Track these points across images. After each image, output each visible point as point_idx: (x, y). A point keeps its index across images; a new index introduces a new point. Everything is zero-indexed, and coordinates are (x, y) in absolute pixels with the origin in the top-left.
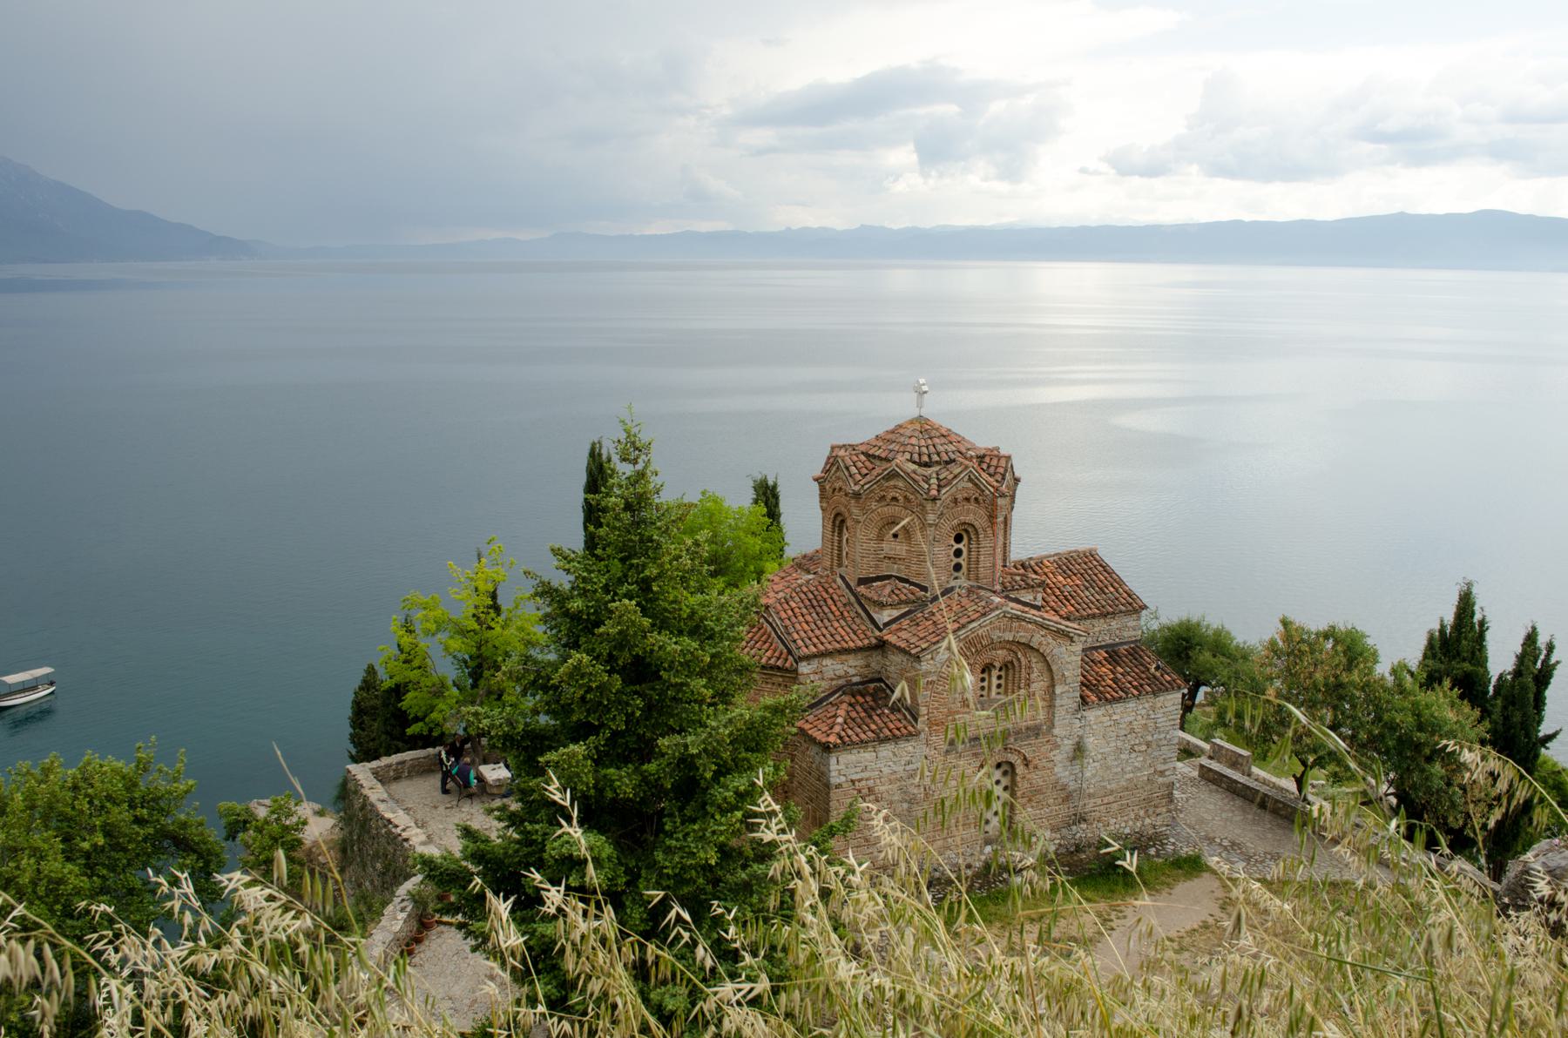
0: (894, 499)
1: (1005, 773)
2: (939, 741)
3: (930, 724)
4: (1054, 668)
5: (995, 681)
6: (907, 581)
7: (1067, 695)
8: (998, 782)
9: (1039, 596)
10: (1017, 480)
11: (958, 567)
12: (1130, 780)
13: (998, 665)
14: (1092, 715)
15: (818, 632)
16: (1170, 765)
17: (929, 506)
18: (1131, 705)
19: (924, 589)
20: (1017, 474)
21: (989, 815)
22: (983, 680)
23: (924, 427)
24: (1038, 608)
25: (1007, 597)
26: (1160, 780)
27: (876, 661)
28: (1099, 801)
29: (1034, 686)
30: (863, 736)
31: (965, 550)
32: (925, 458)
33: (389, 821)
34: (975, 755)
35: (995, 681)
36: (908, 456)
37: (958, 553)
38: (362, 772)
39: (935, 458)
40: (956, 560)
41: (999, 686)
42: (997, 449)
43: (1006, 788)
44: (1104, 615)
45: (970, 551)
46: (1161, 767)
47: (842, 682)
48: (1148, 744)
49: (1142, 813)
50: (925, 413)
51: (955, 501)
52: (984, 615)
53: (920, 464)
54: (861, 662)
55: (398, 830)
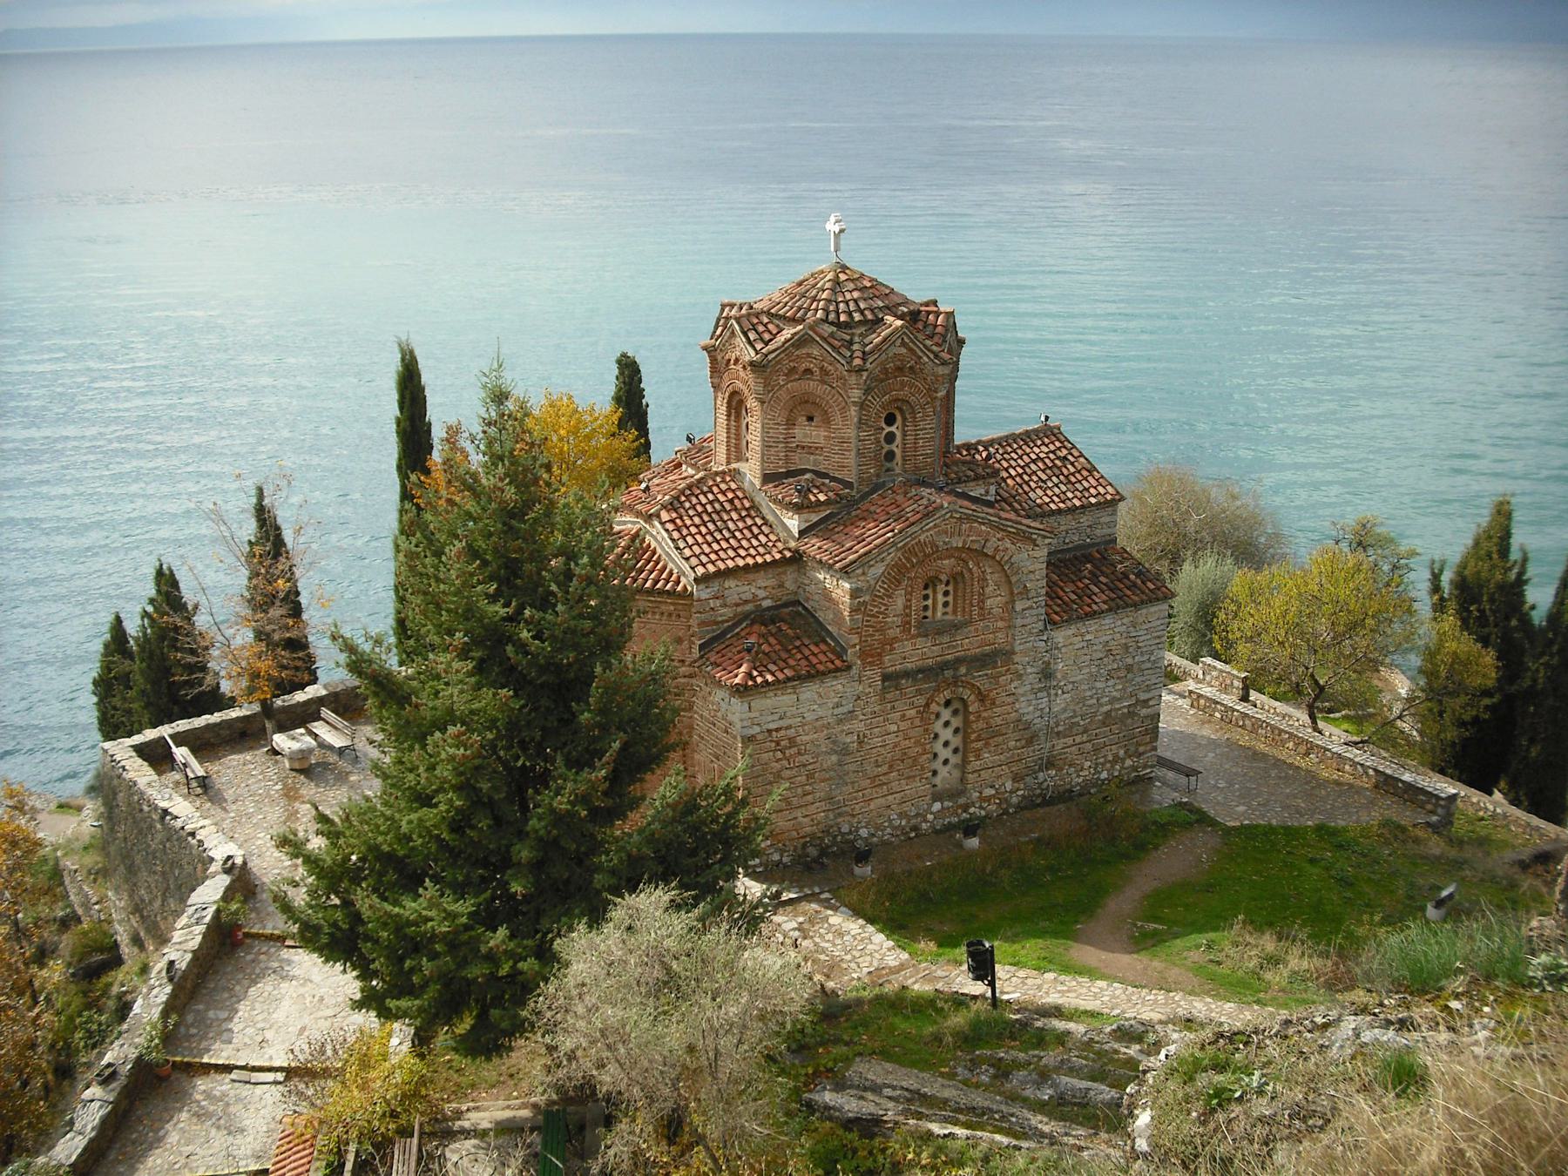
0: (808, 371)
1: (955, 712)
2: (874, 674)
3: (863, 655)
4: (1014, 579)
5: (941, 599)
6: (825, 475)
7: (1031, 612)
8: (947, 724)
9: (992, 489)
10: (961, 342)
11: (890, 456)
13: (944, 578)
14: (1060, 636)
15: (716, 546)
16: (1156, 693)
17: (853, 380)
18: (1107, 621)
19: (849, 485)
21: (937, 765)
22: (926, 597)
23: (843, 279)
24: (990, 504)
25: (952, 492)
26: (1144, 712)
27: (790, 579)
29: (988, 602)
30: (781, 676)
31: (898, 434)
32: (843, 318)
33: (165, 812)
34: (919, 692)
35: (941, 599)
36: (820, 314)
37: (890, 438)
38: (122, 749)
39: (857, 316)
40: (887, 447)
41: (946, 604)
42: (935, 303)
43: (956, 731)
45: (904, 435)
46: (1143, 696)
47: (749, 607)
48: (1129, 668)
49: (1122, 752)
51: (885, 371)
52: (927, 515)
53: (838, 324)
54: (771, 582)
55: (179, 823)
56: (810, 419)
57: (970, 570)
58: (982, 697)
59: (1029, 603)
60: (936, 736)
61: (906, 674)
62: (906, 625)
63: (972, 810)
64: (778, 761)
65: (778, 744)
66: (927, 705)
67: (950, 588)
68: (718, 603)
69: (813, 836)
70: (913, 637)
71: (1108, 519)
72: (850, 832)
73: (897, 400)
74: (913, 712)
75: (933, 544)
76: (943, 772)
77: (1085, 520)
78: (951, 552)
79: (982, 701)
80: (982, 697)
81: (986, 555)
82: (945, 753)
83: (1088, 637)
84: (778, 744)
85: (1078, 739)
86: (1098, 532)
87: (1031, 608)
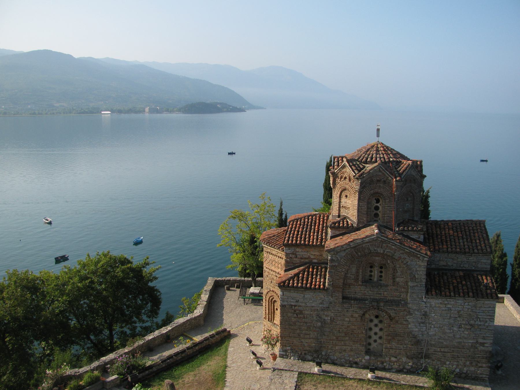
8: (376, 325)
9: (422, 237)
12: (460, 343)
13: (376, 264)
20: (424, 173)
21: (371, 341)
22: (371, 271)
28: (439, 350)
29: (397, 280)
34: (360, 308)
37: (377, 208)
40: (375, 212)
44: (465, 253)
46: (481, 341)
47: (307, 261)
48: (471, 325)
49: (468, 363)
50: (381, 139)
56: (346, 196)
57: (388, 264)
58: (391, 319)
59: (415, 284)
60: (371, 329)
61: (355, 299)
62: (356, 280)
63: (385, 364)
64: (295, 318)
65: (295, 311)
66: (364, 314)
67: (383, 270)
68: (293, 256)
69: (309, 352)
70: (359, 285)
71: (485, 261)
72: (326, 355)
73: (377, 193)
74: (357, 315)
75: (369, 249)
76: (374, 345)
77: (473, 259)
78: (378, 254)
79: (391, 320)
80: (391, 319)
81: (395, 258)
82: (374, 337)
83: (449, 306)
84: (295, 311)
85: (442, 350)
86: (479, 266)
87: (417, 286)
